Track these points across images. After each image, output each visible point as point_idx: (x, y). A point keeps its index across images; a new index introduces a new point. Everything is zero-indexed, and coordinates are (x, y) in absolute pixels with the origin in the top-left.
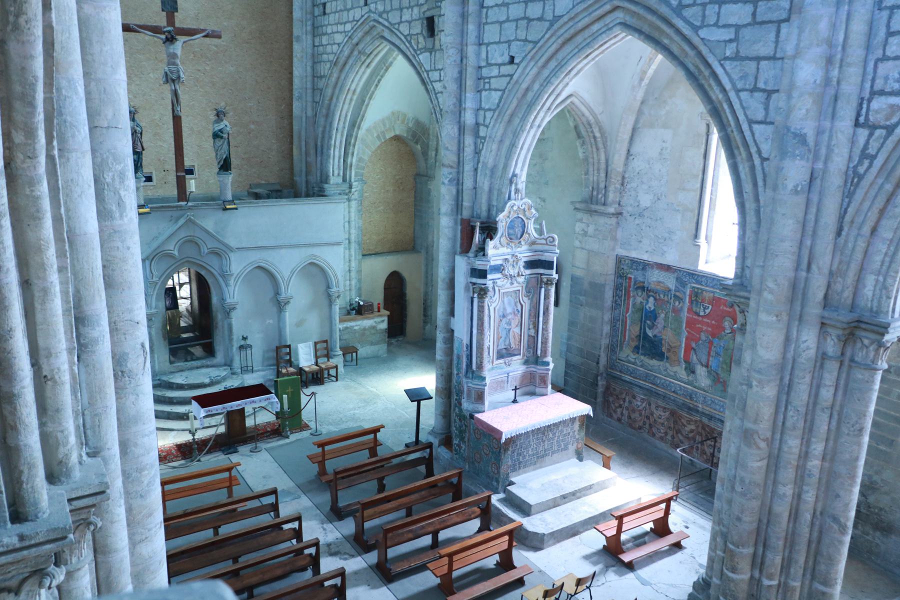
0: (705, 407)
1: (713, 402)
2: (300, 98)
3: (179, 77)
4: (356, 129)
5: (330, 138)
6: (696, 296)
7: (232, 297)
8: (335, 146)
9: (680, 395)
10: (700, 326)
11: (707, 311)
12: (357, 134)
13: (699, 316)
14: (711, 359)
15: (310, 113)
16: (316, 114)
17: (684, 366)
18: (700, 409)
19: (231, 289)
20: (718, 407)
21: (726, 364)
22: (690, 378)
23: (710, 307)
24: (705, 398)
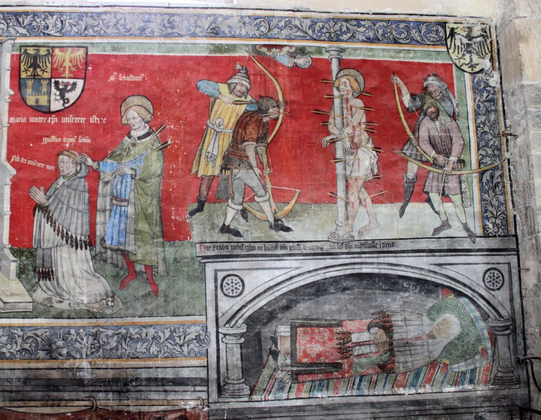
0: (101, 363)
1: (124, 338)
6: (35, 66)
9: (10, 359)
10: (54, 139)
11: (72, 96)
13: (48, 113)
14: (99, 218)
17: (13, 267)
18: (87, 375)
20: (141, 347)
21: (147, 217)
22: (40, 295)
23: (80, 83)
24: (95, 336)
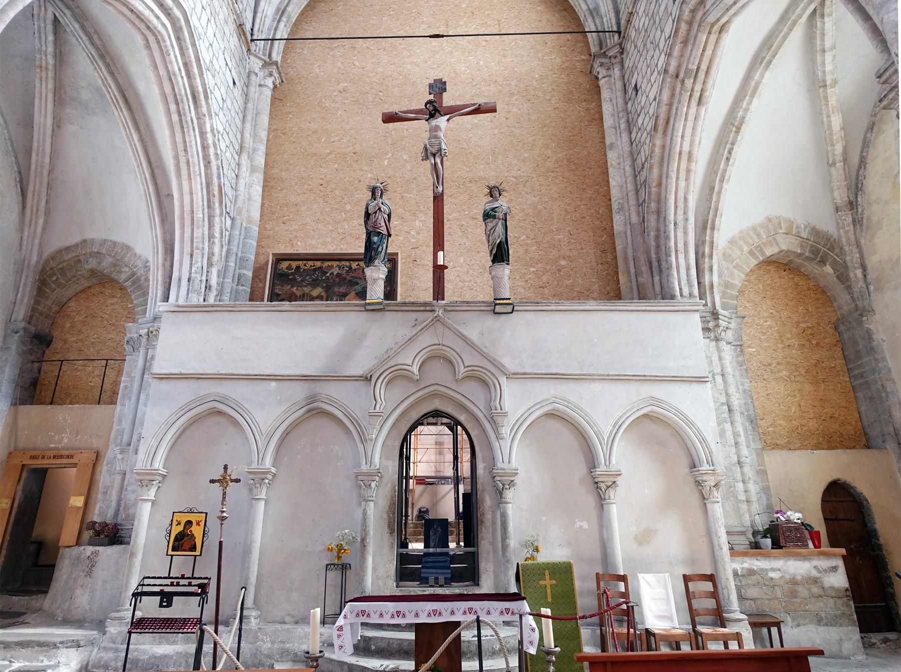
2: (621, 209)
3: (440, 150)
4: (708, 231)
5: (667, 238)
7: (506, 460)
8: (676, 251)
12: (712, 238)
15: (635, 219)
16: (644, 218)
19: (506, 444)
